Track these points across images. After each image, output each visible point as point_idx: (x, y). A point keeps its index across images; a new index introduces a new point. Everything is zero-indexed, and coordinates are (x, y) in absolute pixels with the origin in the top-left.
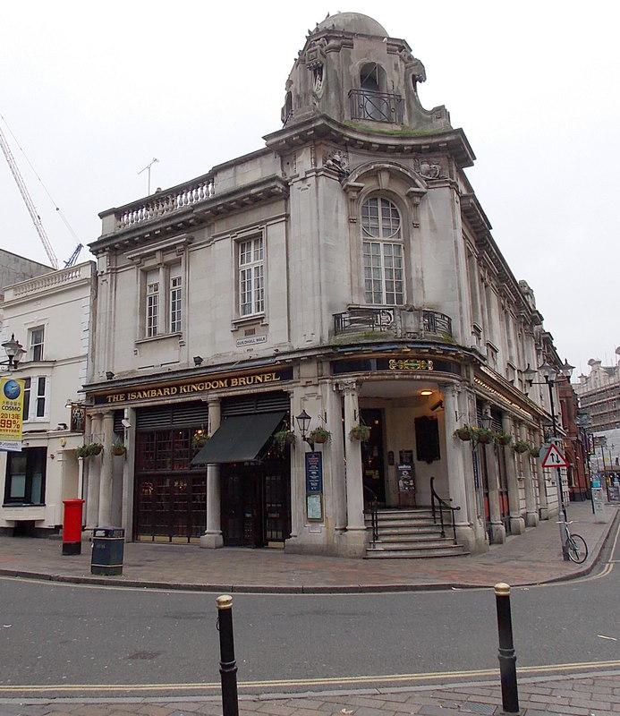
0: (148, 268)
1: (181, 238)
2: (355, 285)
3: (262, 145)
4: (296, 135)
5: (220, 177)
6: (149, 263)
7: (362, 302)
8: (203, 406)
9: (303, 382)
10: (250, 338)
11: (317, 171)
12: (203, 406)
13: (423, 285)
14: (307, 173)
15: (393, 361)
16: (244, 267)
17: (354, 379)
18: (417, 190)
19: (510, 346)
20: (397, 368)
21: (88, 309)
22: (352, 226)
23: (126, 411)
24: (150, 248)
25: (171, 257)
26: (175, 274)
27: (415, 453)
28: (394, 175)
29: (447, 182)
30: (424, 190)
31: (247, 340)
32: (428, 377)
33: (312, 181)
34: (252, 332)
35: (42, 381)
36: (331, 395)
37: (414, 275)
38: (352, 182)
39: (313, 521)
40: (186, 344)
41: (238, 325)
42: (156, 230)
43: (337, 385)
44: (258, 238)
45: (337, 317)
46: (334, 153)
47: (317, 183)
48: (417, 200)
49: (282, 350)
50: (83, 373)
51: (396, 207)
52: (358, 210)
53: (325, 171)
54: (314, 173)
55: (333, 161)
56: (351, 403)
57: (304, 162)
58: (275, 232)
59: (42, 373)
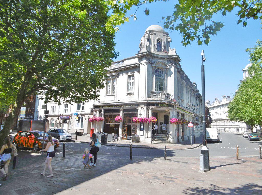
1: (116, 73)
5: (125, 61)
14: (144, 63)
16: (129, 81)
19: (188, 98)
27: (163, 122)
33: (145, 65)
41: (128, 94)
44: (133, 76)
49: (137, 100)
52: (154, 71)
55: (150, 61)
56: (150, 112)
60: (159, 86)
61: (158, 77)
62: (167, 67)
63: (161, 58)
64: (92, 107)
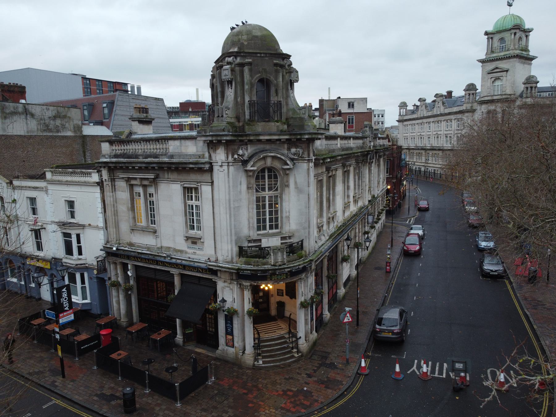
2: (251, 225)
6: (133, 182)
10: (194, 246)
11: (228, 163)
13: (289, 220)
18: (288, 167)
22: (250, 191)
25: (146, 183)
26: (151, 190)
29: (305, 160)
30: (292, 167)
31: (193, 246)
33: (225, 168)
35: (78, 236)
36: (237, 289)
37: (284, 215)
47: (228, 169)
51: (277, 173)
53: (233, 163)
55: (238, 155)
58: (206, 189)
60: (268, 217)
61: (264, 193)
62: (288, 165)
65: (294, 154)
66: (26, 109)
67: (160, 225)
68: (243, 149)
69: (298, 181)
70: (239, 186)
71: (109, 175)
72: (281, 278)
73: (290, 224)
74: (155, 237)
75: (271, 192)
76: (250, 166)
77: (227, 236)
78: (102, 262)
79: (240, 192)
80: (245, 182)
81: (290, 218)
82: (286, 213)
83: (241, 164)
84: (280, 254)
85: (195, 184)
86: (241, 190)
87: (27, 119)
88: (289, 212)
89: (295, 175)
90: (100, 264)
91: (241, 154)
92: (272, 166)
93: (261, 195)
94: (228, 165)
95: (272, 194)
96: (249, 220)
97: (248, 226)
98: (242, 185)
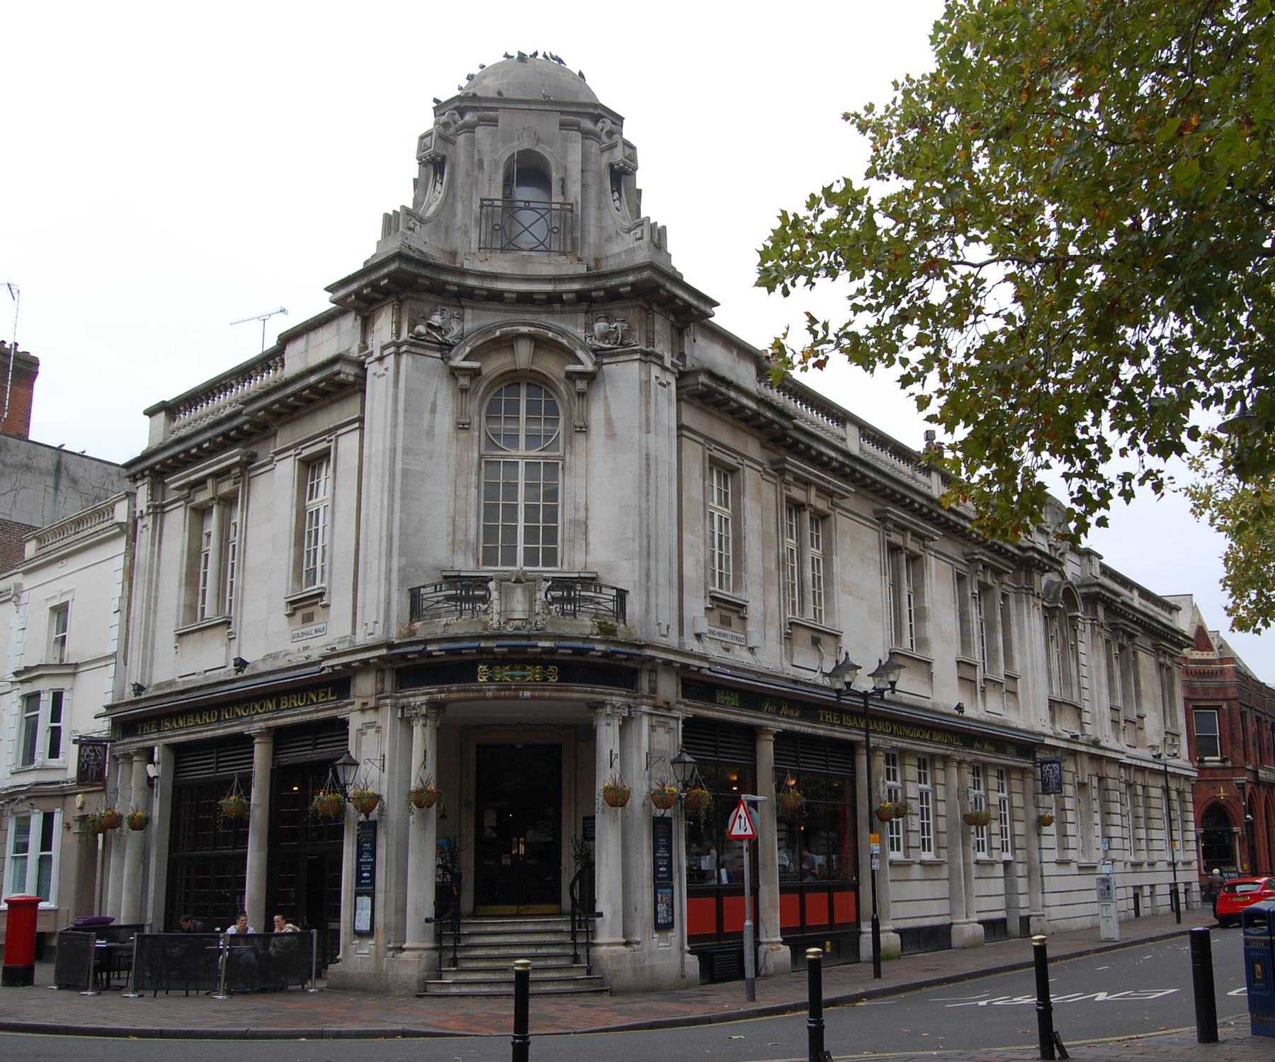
0: (201, 504)
1: (233, 456)
3: (324, 304)
4: (366, 286)
5: (292, 350)
6: (202, 497)
7: (466, 565)
8: (243, 743)
9: (358, 705)
10: (310, 628)
11: (398, 346)
12: (243, 743)
13: (586, 533)
14: (384, 348)
15: (485, 668)
17: (424, 699)
18: (579, 368)
20: (490, 679)
21: (120, 576)
22: (463, 435)
23: (156, 750)
24: (197, 472)
25: (226, 487)
28: (541, 344)
29: (635, 352)
30: (589, 367)
31: (303, 630)
32: (547, 694)
33: (390, 361)
34: (308, 619)
36: (393, 725)
38: (458, 362)
39: (360, 934)
40: (237, 636)
42: (205, 442)
43: (403, 708)
45: (415, 595)
46: (432, 313)
47: (397, 365)
48: (581, 385)
49: (341, 648)
50: (109, 685)
53: (412, 344)
54: (392, 349)
55: (430, 326)
56: (421, 736)
57: (384, 329)
58: (347, 444)
59: (57, 684)
60: (521, 525)
61: (513, 452)
63: (525, 300)
64: (102, 728)
65: (605, 336)
66: (59, 464)
67: (242, 602)
68: (447, 315)
69: (615, 415)
70: (427, 416)
71: (152, 495)
72: (524, 677)
73: (587, 545)
74: (226, 640)
75: (533, 453)
76: (463, 356)
77: (380, 558)
78: (94, 751)
79: (431, 432)
80: (450, 408)
81: (590, 527)
82: (576, 509)
83: (439, 355)
84: (519, 594)
85: (325, 439)
86: (432, 427)
87: (56, 489)
88: (587, 510)
89: (606, 398)
90: (88, 756)
91: (436, 325)
92: (533, 367)
93: (503, 456)
94: (398, 355)
95: (537, 457)
96: (454, 521)
97: (450, 539)
98: (438, 417)
